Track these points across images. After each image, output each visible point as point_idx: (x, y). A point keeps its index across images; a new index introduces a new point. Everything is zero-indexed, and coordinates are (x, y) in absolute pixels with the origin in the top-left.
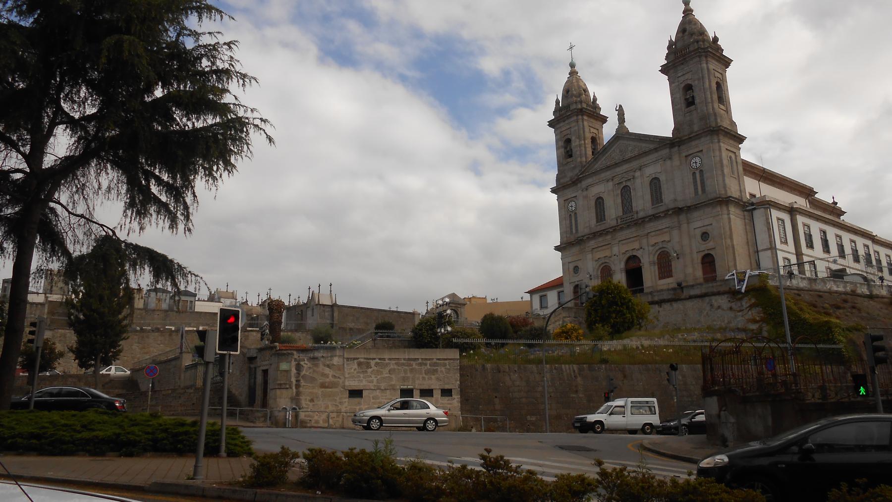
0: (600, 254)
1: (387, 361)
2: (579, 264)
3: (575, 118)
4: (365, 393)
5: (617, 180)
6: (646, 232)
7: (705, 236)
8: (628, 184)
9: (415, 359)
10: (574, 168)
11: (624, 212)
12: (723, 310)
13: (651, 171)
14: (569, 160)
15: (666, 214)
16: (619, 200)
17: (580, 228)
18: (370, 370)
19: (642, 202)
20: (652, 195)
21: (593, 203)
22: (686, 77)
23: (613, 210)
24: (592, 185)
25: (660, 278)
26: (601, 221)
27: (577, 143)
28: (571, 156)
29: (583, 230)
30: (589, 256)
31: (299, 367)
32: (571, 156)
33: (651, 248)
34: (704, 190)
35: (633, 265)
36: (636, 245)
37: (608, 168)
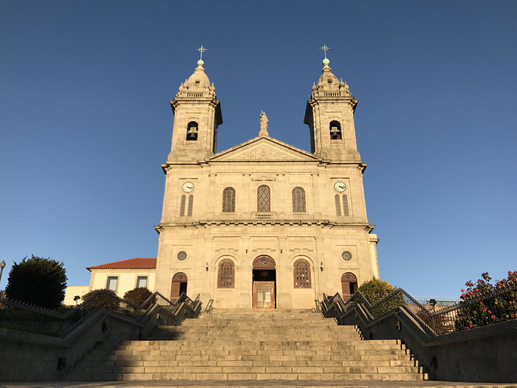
3: (207, 106)
5: (254, 176)
7: (347, 255)
8: (268, 184)
10: (199, 151)
11: (259, 209)
13: (296, 180)
16: (255, 197)
19: (282, 204)
22: (336, 114)
23: (246, 204)
25: (296, 287)
26: (229, 211)
27: (205, 129)
29: (198, 215)
30: (209, 244)
34: (347, 213)
35: (263, 266)
36: (272, 246)
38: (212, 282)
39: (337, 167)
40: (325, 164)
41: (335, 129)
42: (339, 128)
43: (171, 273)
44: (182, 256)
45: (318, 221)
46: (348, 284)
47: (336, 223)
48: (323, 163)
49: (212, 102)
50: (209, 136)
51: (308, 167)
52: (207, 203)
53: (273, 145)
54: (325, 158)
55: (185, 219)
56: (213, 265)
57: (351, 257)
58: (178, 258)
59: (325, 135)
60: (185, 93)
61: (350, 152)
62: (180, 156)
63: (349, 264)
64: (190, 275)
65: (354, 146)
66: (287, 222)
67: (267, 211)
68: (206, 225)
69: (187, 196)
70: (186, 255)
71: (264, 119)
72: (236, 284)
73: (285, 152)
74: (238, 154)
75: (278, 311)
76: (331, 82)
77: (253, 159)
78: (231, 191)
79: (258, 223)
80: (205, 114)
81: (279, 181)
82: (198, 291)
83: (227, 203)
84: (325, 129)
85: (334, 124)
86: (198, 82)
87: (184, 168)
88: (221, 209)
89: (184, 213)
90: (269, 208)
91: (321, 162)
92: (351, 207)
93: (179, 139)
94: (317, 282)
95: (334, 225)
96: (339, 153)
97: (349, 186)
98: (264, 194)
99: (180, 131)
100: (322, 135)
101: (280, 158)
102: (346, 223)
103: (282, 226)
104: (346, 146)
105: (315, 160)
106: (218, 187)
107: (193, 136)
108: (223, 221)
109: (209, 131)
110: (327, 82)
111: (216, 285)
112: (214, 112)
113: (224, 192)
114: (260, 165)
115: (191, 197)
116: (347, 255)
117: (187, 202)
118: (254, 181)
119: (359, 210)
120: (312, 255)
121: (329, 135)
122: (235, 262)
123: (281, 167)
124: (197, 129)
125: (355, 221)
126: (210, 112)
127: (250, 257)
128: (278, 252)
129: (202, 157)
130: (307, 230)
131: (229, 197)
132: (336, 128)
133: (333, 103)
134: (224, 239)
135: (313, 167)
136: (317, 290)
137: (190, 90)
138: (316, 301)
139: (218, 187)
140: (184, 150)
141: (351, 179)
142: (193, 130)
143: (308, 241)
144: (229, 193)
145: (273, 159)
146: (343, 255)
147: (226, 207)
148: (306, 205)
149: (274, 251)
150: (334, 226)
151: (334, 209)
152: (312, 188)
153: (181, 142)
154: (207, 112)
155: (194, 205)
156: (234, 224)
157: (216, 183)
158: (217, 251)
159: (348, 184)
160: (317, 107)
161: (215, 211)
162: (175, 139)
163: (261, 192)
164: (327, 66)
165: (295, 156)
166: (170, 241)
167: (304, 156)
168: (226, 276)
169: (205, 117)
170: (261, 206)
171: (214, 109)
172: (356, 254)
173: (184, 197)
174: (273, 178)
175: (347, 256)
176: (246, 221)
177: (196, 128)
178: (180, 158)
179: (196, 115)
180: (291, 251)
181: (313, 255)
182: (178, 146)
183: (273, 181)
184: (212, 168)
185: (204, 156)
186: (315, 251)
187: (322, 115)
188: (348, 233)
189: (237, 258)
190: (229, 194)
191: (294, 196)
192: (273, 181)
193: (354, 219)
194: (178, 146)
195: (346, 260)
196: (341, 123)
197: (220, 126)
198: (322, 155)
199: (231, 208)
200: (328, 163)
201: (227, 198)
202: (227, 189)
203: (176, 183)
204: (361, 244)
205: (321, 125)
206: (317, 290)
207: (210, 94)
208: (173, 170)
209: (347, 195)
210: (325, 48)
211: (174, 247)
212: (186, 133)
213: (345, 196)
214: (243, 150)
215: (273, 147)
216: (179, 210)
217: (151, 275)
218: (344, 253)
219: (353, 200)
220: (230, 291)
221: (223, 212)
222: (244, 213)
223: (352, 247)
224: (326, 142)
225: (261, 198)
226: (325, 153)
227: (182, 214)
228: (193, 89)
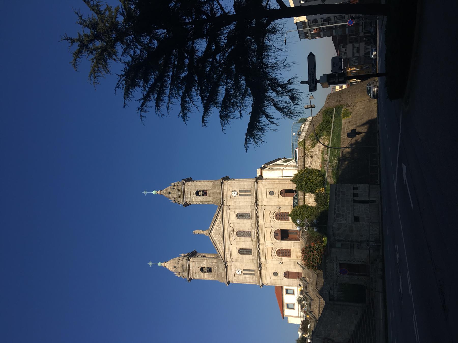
0: (269, 253)
1: (336, 207)
4: (356, 215)
5: (232, 239)
7: (272, 193)
8: (235, 231)
9: (336, 198)
12: (312, 161)
14: (212, 270)
16: (243, 239)
18: (342, 213)
19: (246, 225)
20: (245, 219)
21: (241, 256)
22: (192, 193)
23: (247, 243)
24: (230, 255)
26: (251, 252)
27: (205, 263)
28: (211, 268)
29: (254, 266)
30: (269, 262)
31: (339, 241)
32: (211, 268)
33: (272, 223)
34: (249, 191)
35: (279, 236)
36: (269, 231)
38: (288, 260)
41: (200, 193)
42: (200, 191)
50: (208, 261)
61: (215, 188)
62: (221, 276)
64: (284, 270)
65: (210, 183)
69: (244, 272)
71: (197, 232)
72: (289, 248)
74: (220, 247)
77: (222, 239)
80: (195, 264)
81: (234, 226)
85: (197, 193)
86: (174, 267)
88: (251, 256)
90: (249, 231)
91: (222, 204)
95: (257, 200)
96: (215, 193)
99: (206, 276)
105: (221, 209)
107: (209, 270)
109: (205, 261)
111: (290, 258)
113: (241, 254)
115: (244, 270)
117: (246, 272)
119: (247, 184)
121: (205, 197)
123: (226, 224)
126: (194, 261)
129: (222, 265)
131: (244, 252)
135: (225, 208)
144: (241, 251)
145: (221, 228)
155: (249, 269)
162: (211, 279)
163: (240, 235)
164: (158, 192)
166: (268, 280)
168: (285, 253)
169: (198, 264)
173: (244, 274)
178: (223, 277)
179: (197, 268)
184: (228, 260)
190: (242, 251)
200: (222, 200)
202: (239, 252)
203: (236, 277)
204: (265, 186)
208: (230, 280)
210: (145, 192)
213: (240, 191)
217: (285, 288)
222: (252, 244)
227: (253, 274)
228: (180, 270)
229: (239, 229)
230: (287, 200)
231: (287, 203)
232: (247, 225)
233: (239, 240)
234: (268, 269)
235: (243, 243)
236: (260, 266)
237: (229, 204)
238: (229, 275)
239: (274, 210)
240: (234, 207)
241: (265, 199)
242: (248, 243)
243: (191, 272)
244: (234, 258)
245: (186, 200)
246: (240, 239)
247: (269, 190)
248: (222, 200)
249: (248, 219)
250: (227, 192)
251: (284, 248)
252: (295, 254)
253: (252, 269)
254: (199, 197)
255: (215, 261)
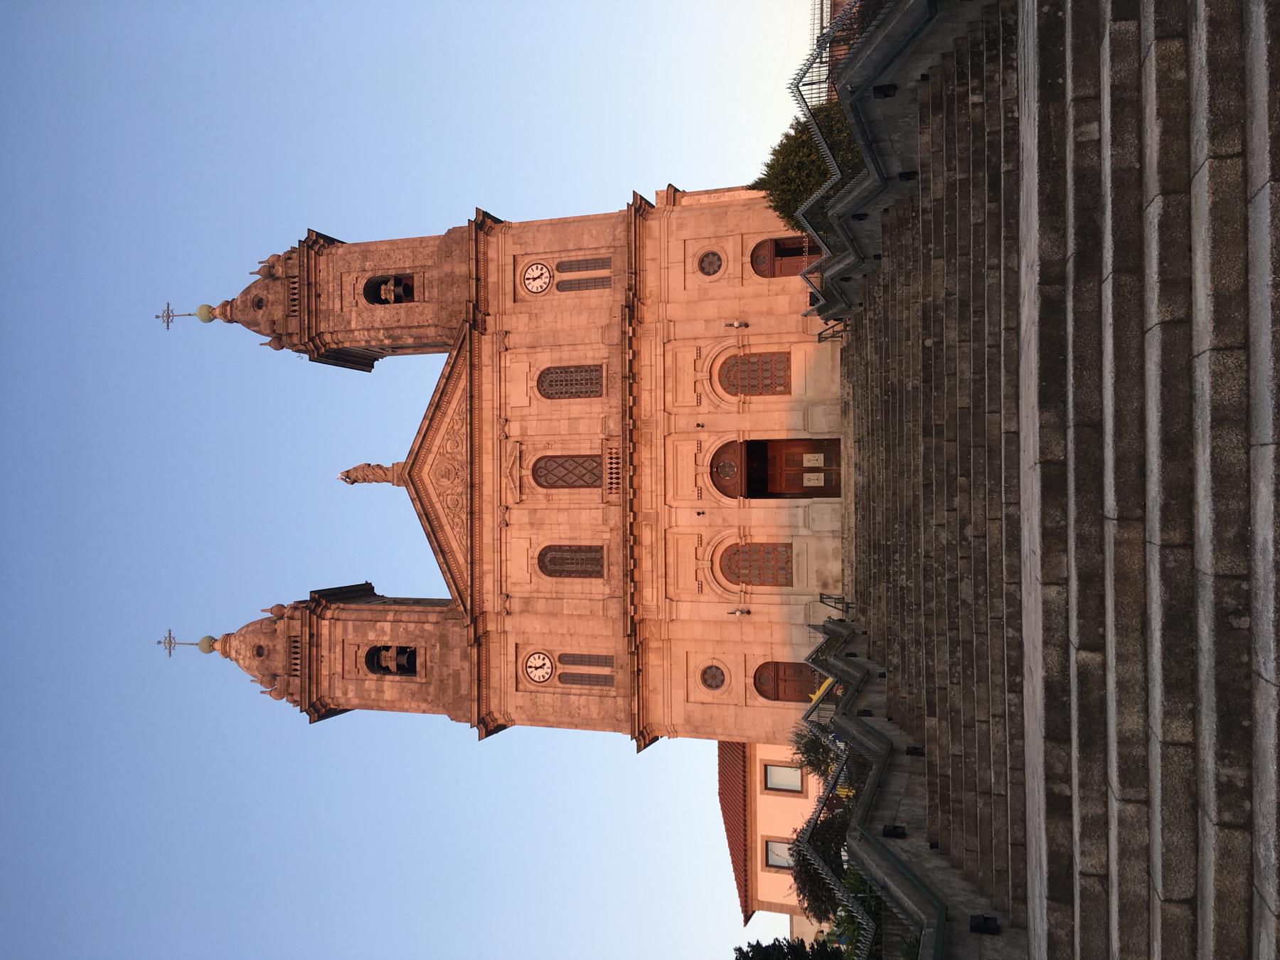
2: (701, 661)
6: (660, 416)
7: (709, 263)
8: (530, 460)
10: (444, 642)
13: (519, 390)
14: (419, 660)
15: (629, 342)
16: (563, 495)
17: (600, 649)
19: (582, 426)
21: (548, 583)
22: (348, 288)
23: (581, 517)
24: (501, 580)
25: (788, 391)
26: (599, 561)
27: (387, 626)
30: (685, 610)
35: (736, 471)
36: (688, 449)
37: (472, 532)
38: (777, 599)
39: (486, 287)
40: (480, 316)
41: (387, 291)
43: (756, 703)
44: (714, 677)
45: (624, 333)
46: (779, 262)
47: (630, 289)
48: (475, 320)
49: (312, 612)
50: (404, 617)
51: (486, 360)
52: (580, 616)
53: (429, 451)
54: (464, 316)
55: (620, 671)
56: (736, 598)
57: (714, 254)
58: (718, 687)
59: (403, 315)
60: (288, 684)
62: (457, 691)
63: (731, 258)
66: (629, 412)
67: (600, 464)
68: (636, 618)
69: (561, 669)
70: (710, 667)
73: (447, 420)
75: (846, 434)
76: (261, 300)
77: (464, 501)
78: (549, 556)
79: (631, 486)
80: (345, 628)
81: (524, 434)
82: (799, 635)
83: (579, 568)
84: (388, 317)
85: (373, 292)
87: (488, 679)
88: (597, 582)
89: (606, 677)
91: (474, 326)
92: (588, 252)
93: (413, 695)
94: (775, 339)
97: (534, 257)
98: (556, 472)
100: (402, 323)
101: (464, 430)
102: (630, 263)
103: (639, 423)
104: (430, 263)
106: (538, 591)
107: (404, 660)
108: (625, 575)
109: (390, 617)
110: (261, 312)
112: (342, 605)
113: (550, 574)
114: (481, 483)
115: (564, 659)
116: (709, 263)
118: (524, 497)
120: (710, 350)
122: (727, 543)
123: (487, 428)
124: (387, 648)
125: (623, 242)
126: (343, 615)
127: (715, 505)
128: (703, 436)
130: (647, 362)
131: (563, 561)
132: (383, 287)
133: (318, 296)
134: (671, 572)
135: (487, 346)
136: (793, 338)
137: (280, 671)
138: (820, 341)
139: (538, 591)
140: (441, 681)
141: (518, 250)
142: (389, 660)
143: (675, 359)
144: (553, 561)
145: (464, 448)
146: (708, 274)
147: (589, 568)
148: (584, 363)
149: (700, 444)
150: (635, 295)
151: (595, 297)
152: (539, 350)
153: (420, 689)
154: (340, 624)
155: (585, 652)
156: (632, 548)
157: (526, 595)
158: (701, 590)
159: (528, 259)
160: (328, 338)
161: (600, 597)
165: (458, 393)
167: (457, 370)
169: (356, 629)
170: (586, 478)
171: (333, 606)
172: (706, 242)
173: (564, 678)
174: (513, 448)
175: (711, 264)
176: (625, 517)
177: (384, 652)
178: (464, 691)
179: (350, 651)
180: (699, 402)
181: (709, 348)
182: (430, 698)
183: (524, 447)
184: (488, 606)
185: (457, 629)
186: (701, 343)
187: (349, 322)
188: (653, 260)
189: (717, 539)
191: (561, 395)
192: (524, 447)
193: (618, 243)
194: (430, 698)
195: (719, 267)
196: (369, 275)
197: (378, 591)
198: (454, 324)
199: (592, 555)
200: (476, 307)
201: (568, 567)
204: (681, 227)
205: (377, 325)
206: (793, 338)
207: (291, 618)
209: (557, 261)
211: (692, 699)
212: (397, 678)
214: (441, 526)
215: (435, 449)
216: (596, 690)
218: (702, 269)
219: (571, 247)
220: (798, 555)
221: (602, 576)
222: (605, 522)
223: (690, 251)
224: (421, 314)
225: (566, 478)
226: (451, 315)
227: (607, 681)
229: (548, 445)
230: (784, 291)
231: (782, 303)
232: (583, 427)
233: (543, 504)
234: (679, 651)
235: (563, 517)
236: (634, 630)
237: (506, 328)
238: (494, 681)
239: (718, 339)
240: (528, 340)
241: (677, 292)
242: (585, 517)
243: (325, 672)
244: (516, 592)
245: (323, 327)
246: (547, 495)
247: (696, 249)
248: (476, 307)
249: (588, 394)
250: (501, 269)
251: (757, 540)
252: (814, 566)
253: (602, 651)
254: (380, 310)
255: (433, 618)
